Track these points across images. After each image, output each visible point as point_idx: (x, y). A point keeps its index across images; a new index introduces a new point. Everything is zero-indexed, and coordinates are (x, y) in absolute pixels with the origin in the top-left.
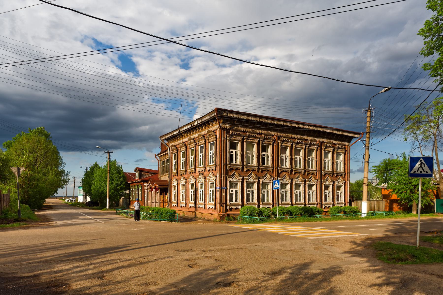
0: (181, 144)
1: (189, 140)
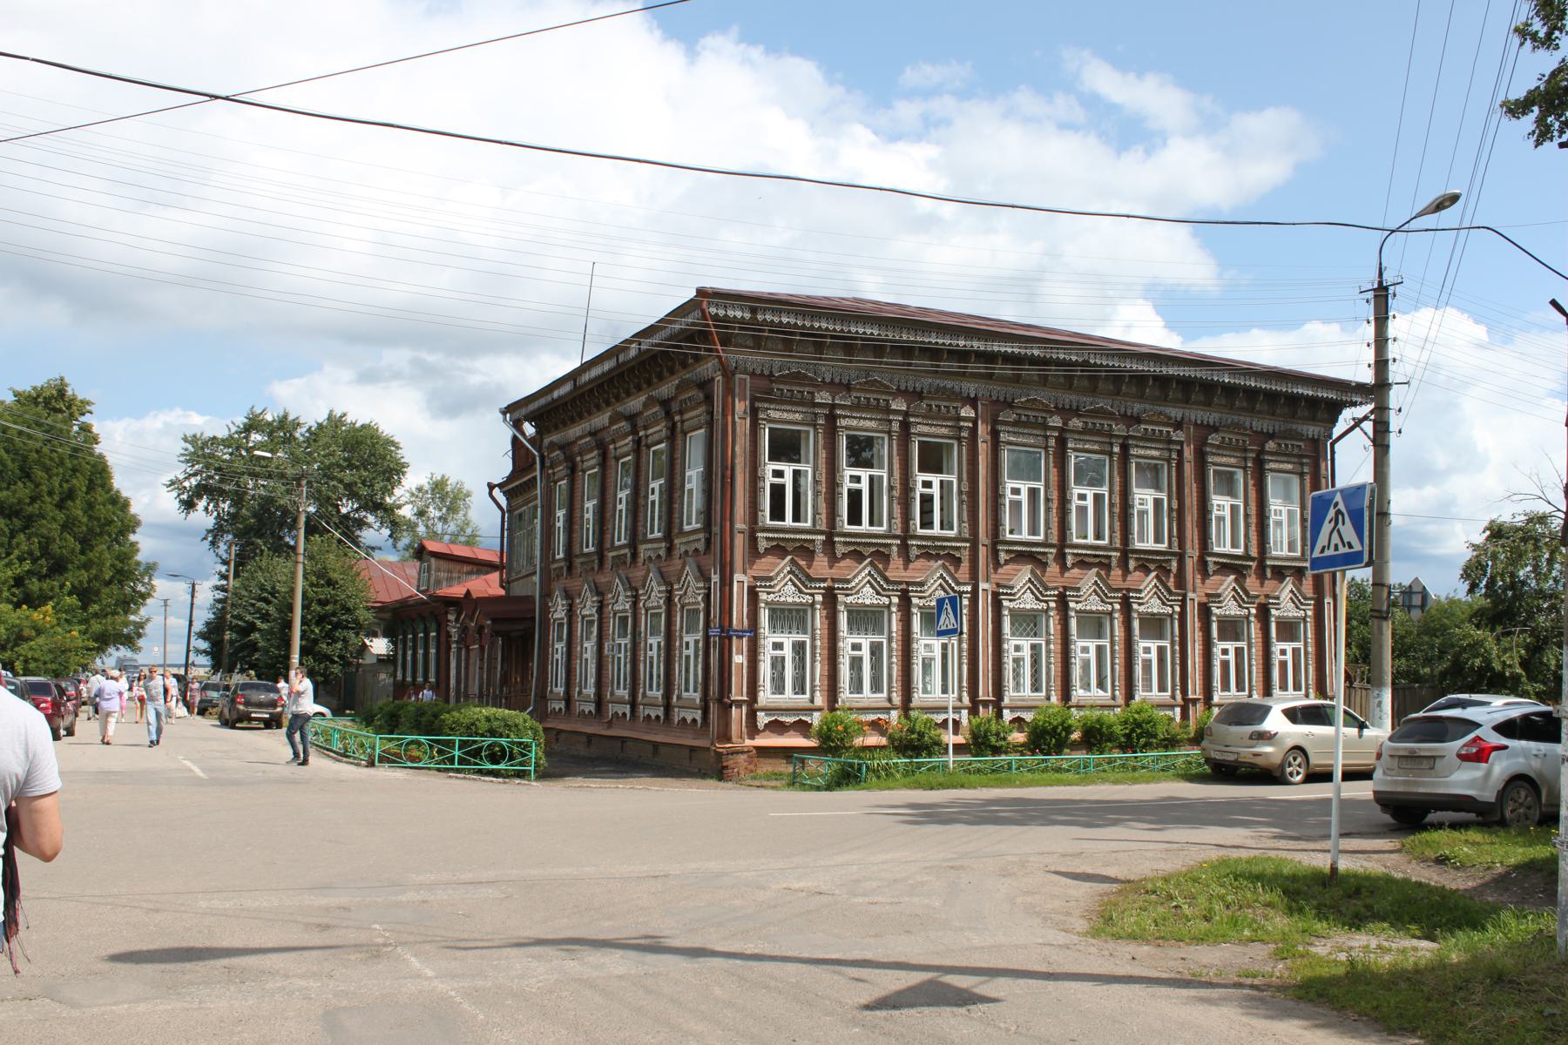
0: (583, 441)
1: (613, 421)
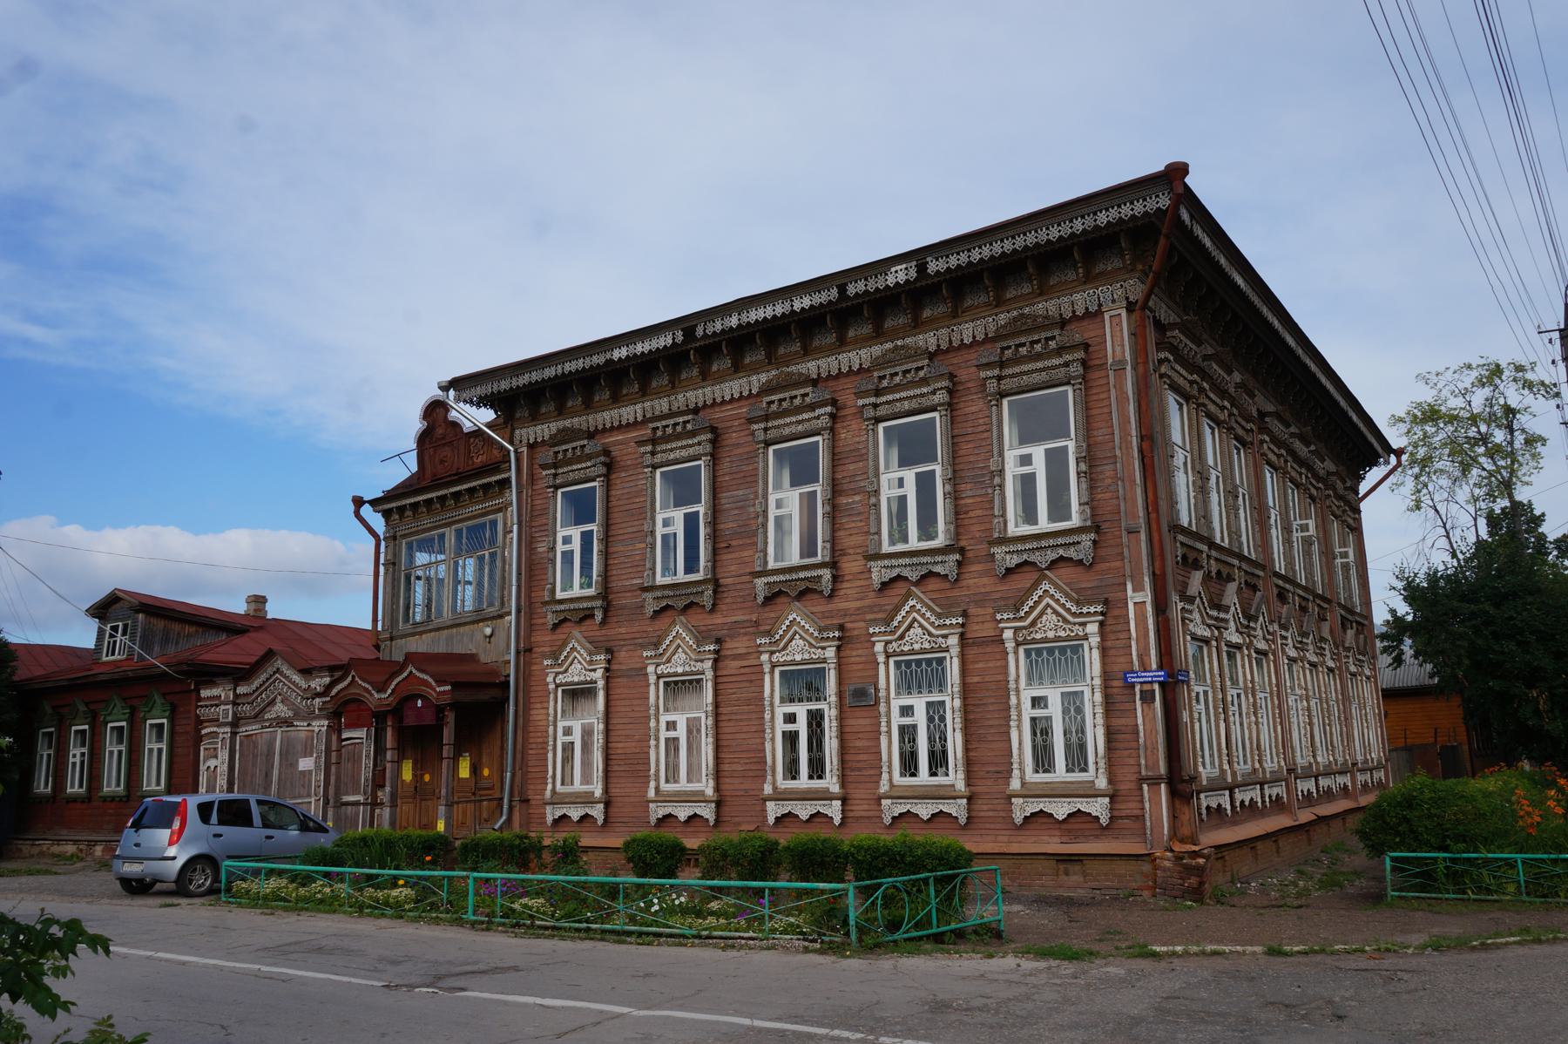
0: (672, 422)
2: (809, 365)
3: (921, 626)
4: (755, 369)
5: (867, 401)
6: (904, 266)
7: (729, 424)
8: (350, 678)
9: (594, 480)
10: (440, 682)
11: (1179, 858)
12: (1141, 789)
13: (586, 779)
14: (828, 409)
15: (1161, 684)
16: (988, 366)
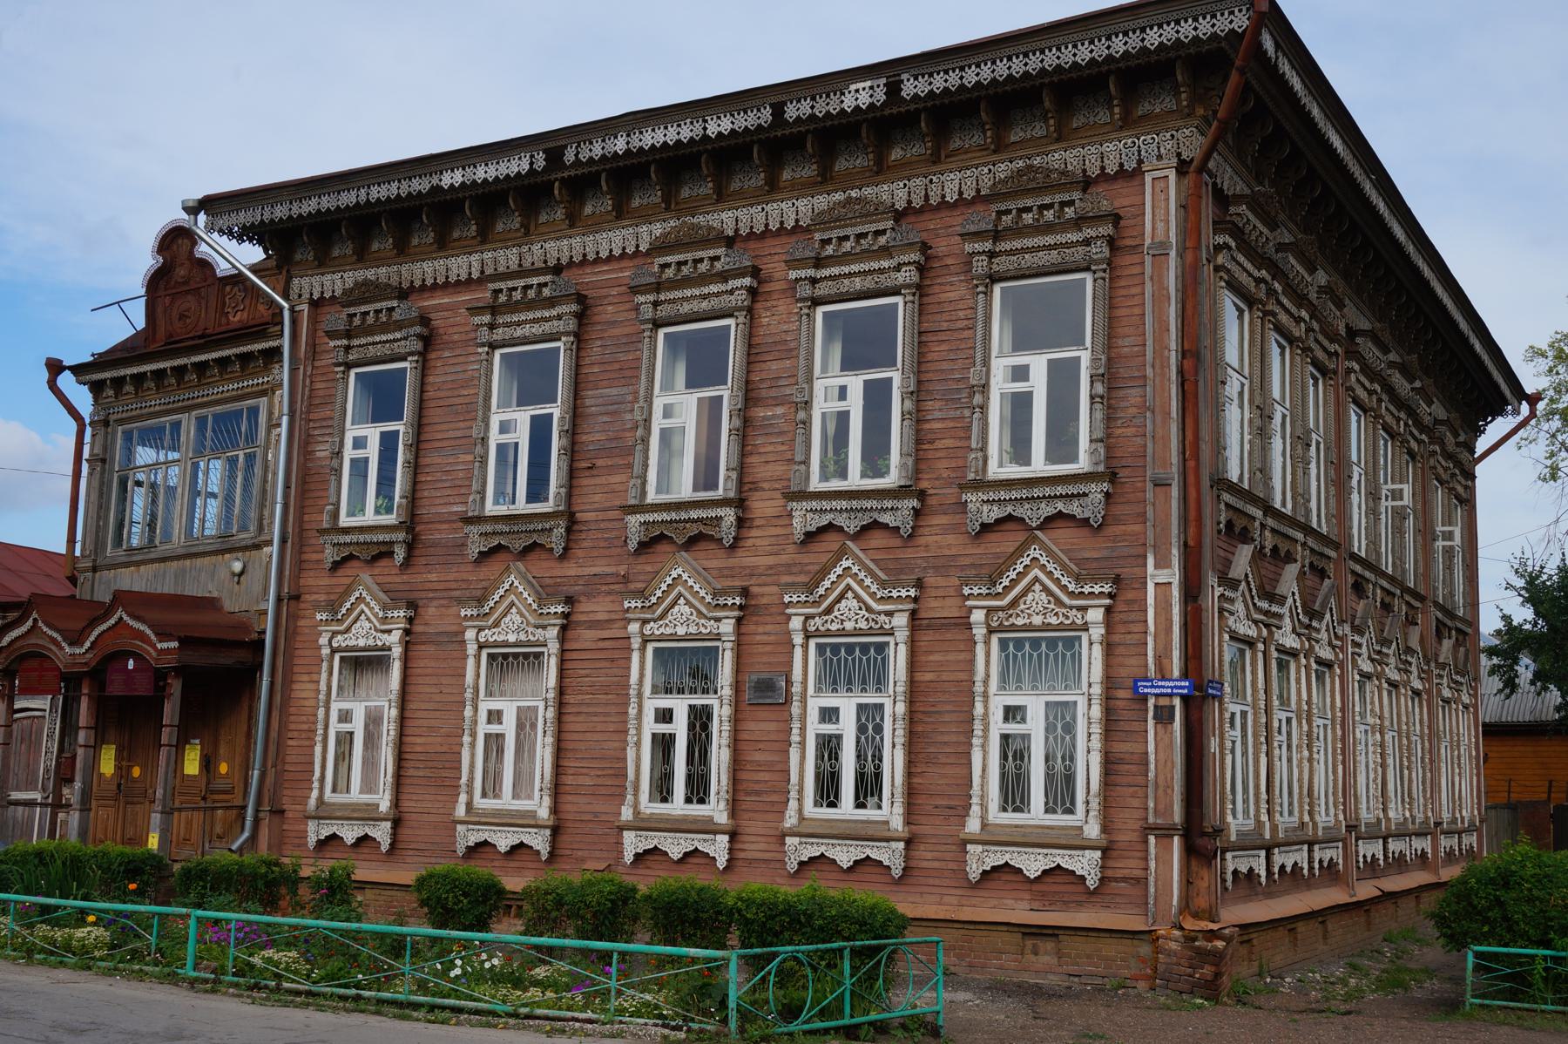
0: (521, 283)
2: (724, 216)
3: (857, 597)
4: (646, 217)
5: (803, 273)
6: (868, 84)
7: (604, 292)
8: (30, 623)
9: (404, 359)
10: (162, 636)
11: (1190, 938)
12: (1146, 842)
13: (369, 785)
14: (747, 281)
15: (1183, 697)
16: (977, 235)
